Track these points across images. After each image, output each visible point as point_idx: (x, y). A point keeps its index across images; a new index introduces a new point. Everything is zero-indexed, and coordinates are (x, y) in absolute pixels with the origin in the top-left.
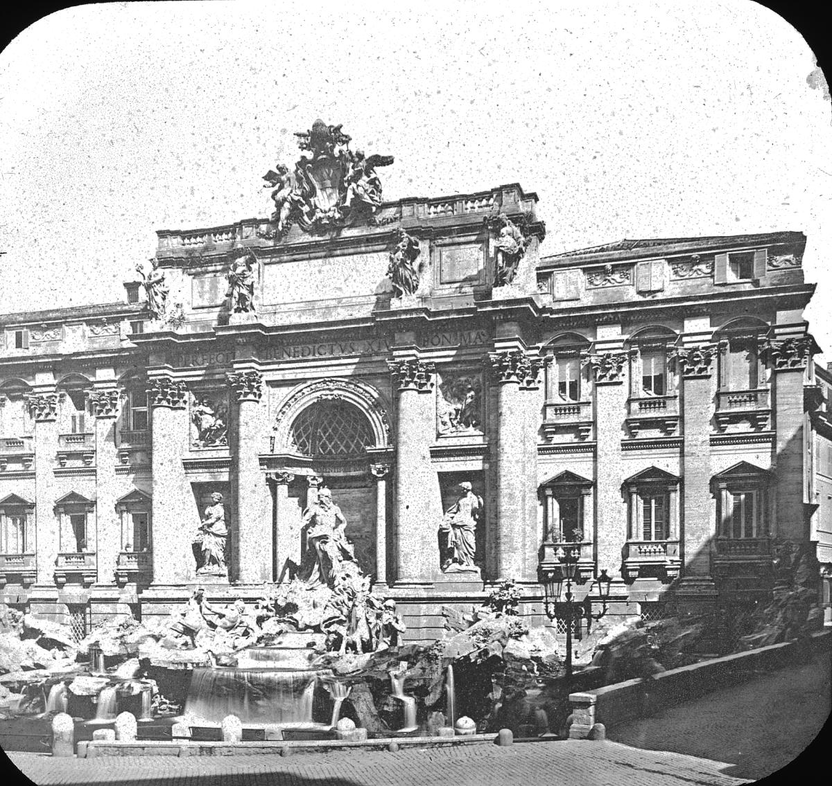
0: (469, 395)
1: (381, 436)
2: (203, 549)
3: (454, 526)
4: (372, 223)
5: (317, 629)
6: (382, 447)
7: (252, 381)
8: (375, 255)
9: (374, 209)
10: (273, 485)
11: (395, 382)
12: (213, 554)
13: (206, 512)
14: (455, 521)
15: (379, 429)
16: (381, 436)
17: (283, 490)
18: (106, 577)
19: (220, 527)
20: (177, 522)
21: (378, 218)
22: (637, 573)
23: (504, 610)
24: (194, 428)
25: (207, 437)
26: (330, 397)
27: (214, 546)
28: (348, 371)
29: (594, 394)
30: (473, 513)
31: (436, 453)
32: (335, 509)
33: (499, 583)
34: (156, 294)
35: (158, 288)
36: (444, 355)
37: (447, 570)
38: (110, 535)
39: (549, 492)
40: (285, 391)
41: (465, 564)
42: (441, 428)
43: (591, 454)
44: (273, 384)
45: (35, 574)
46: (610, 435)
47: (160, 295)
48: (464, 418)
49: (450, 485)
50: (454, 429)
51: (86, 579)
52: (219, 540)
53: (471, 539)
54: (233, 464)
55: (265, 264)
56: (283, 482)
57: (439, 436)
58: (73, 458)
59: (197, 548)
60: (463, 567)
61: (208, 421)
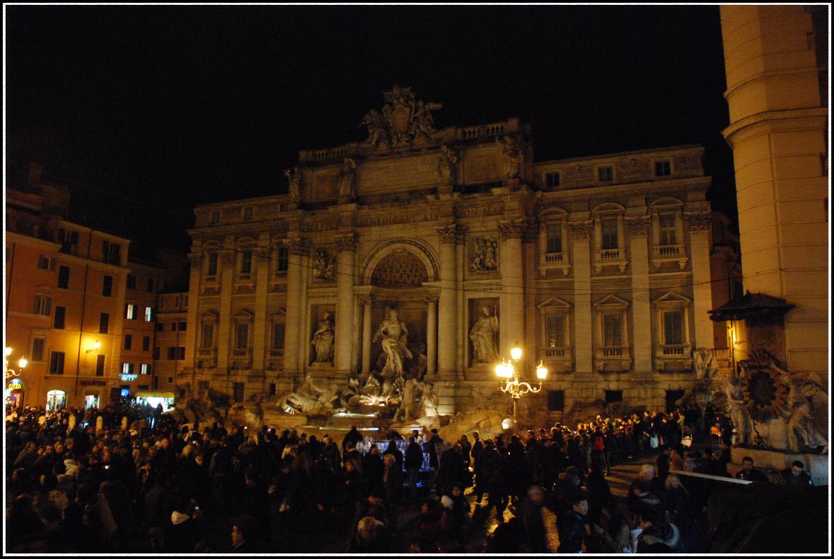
0: (489, 249)
17: (367, 309)
24: (315, 272)
50: (478, 271)
59: (313, 348)
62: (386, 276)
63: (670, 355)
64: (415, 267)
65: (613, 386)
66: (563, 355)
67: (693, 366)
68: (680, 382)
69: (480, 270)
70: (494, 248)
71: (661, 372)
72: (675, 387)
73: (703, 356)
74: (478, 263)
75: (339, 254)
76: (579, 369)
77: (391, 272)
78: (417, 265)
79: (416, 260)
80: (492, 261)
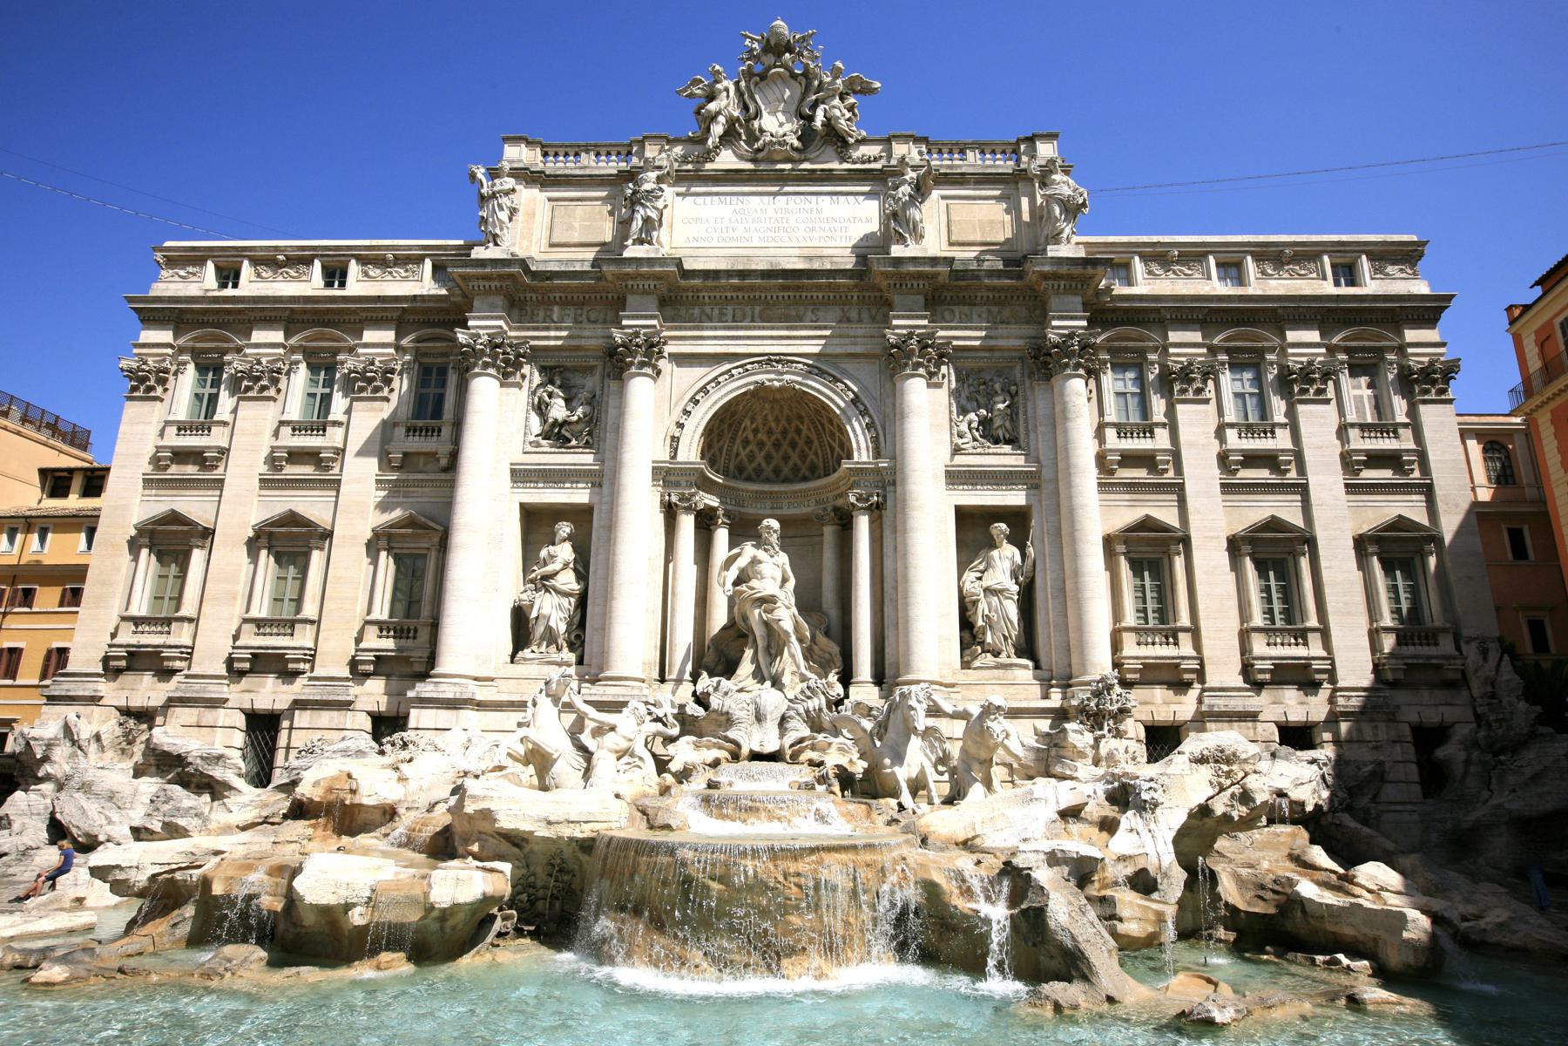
1: (863, 445)
2: (534, 615)
3: (987, 590)
4: (843, 160)
5: (774, 757)
6: (864, 458)
7: (652, 349)
8: (851, 198)
9: (851, 140)
10: (670, 513)
11: (894, 362)
12: (552, 624)
13: (543, 553)
14: (985, 583)
15: (861, 438)
16: (863, 445)
18: (334, 662)
19: (567, 580)
20: (485, 570)
21: (856, 154)
22: (1268, 676)
23: (1106, 728)
24: (535, 421)
25: (557, 434)
26: (777, 384)
27: (553, 611)
28: (814, 347)
29: (1171, 412)
30: (1014, 575)
31: (956, 478)
32: (783, 558)
33: (1088, 683)
34: (501, 208)
35: (504, 200)
36: (969, 336)
37: (977, 663)
38: (350, 592)
39: (1121, 548)
40: (695, 376)
41: (1004, 654)
42: (960, 441)
43: (1175, 497)
44: (682, 360)
45: (188, 653)
46: (1201, 474)
47: (507, 212)
48: (989, 432)
49: (974, 530)
51: (290, 666)
52: (565, 601)
53: (1012, 610)
54: (605, 479)
55: (678, 194)
56: (688, 510)
57: (957, 450)
58: (304, 463)
60: (1003, 659)
61: (558, 410)
62: (720, 450)
63: (1411, 648)
64: (792, 435)
65: (1296, 715)
66: (1176, 644)
67: (1463, 672)
68: (1441, 709)
69: (975, 439)
70: (1012, 397)
71: (1394, 685)
72: (1432, 716)
73: (1484, 653)
74: (975, 425)
75: (613, 385)
76: (1212, 681)
77: (733, 439)
78: (798, 431)
79: (800, 418)
80: (1008, 424)
